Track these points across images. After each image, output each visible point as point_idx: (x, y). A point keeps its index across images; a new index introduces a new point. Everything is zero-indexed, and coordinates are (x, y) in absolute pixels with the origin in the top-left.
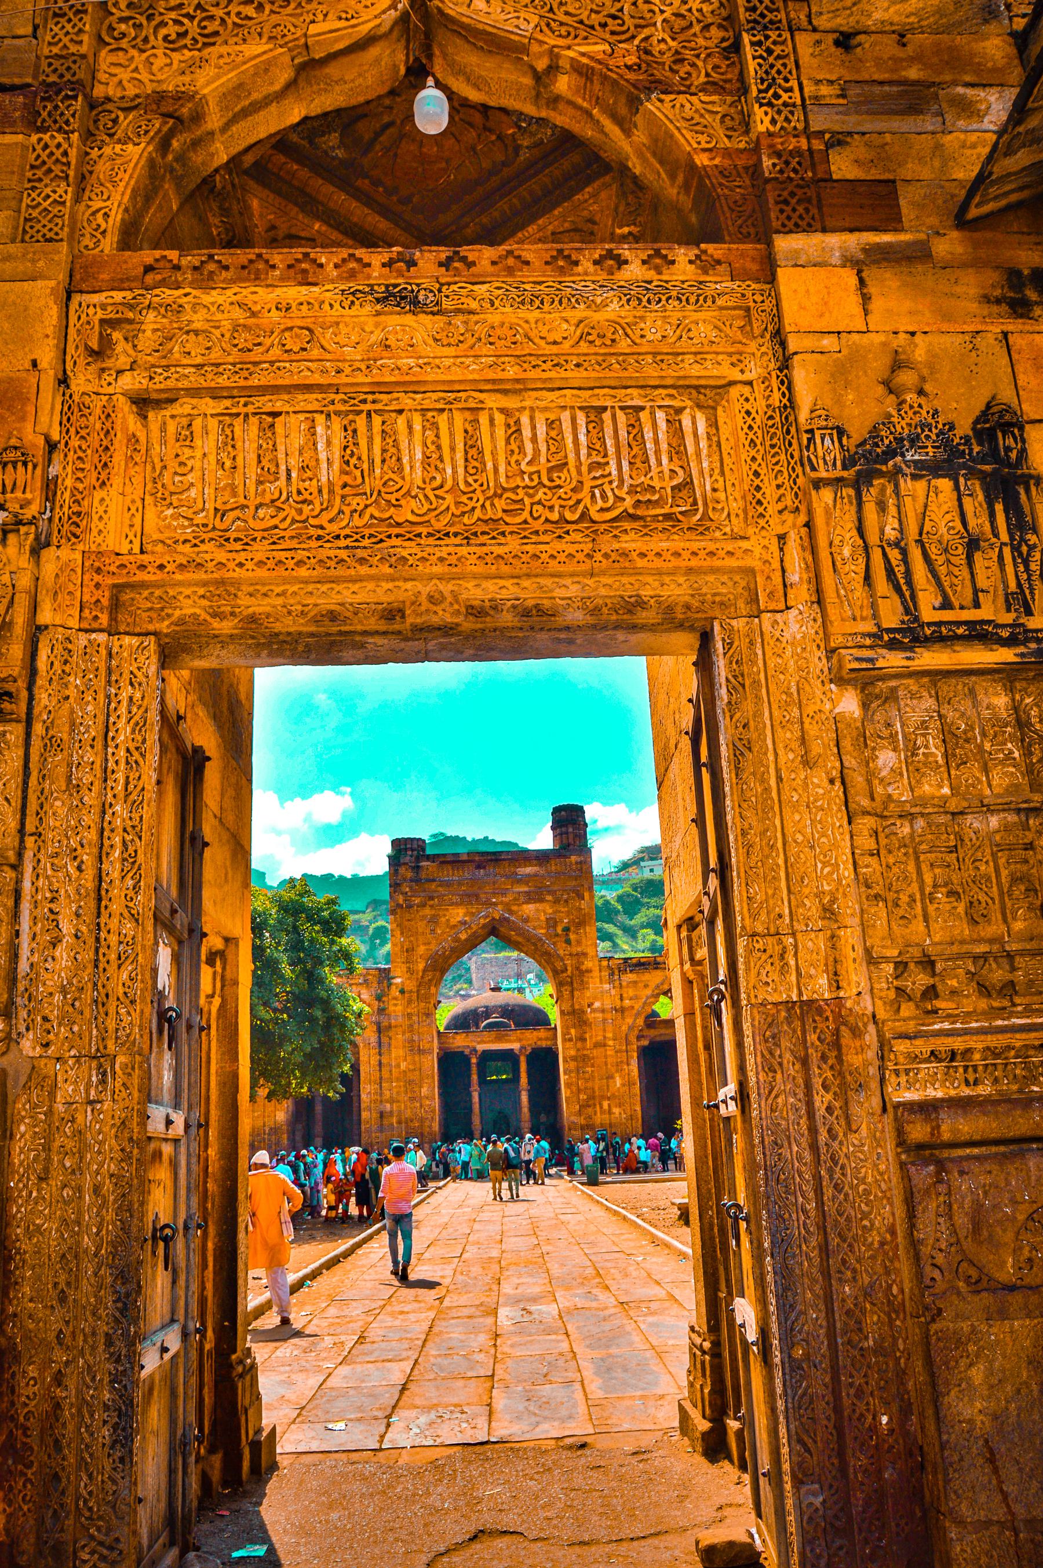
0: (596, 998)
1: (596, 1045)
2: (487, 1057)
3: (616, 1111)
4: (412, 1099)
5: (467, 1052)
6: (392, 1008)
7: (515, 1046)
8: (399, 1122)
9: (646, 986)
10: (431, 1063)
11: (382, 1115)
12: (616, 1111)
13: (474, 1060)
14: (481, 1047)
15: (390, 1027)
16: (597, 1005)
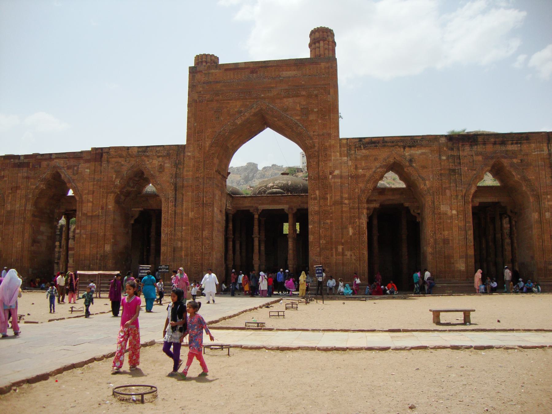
0: (336, 168)
1: (335, 203)
2: (265, 213)
3: (348, 253)
4: (196, 239)
6: (185, 173)
7: (285, 207)
8: (186, 255)
9: (376, 159)
11: (174, 250)
12: (348, 253)
13: (256, 216)
14: (261, 207)
15: (183, 187)
16: (337, 172)
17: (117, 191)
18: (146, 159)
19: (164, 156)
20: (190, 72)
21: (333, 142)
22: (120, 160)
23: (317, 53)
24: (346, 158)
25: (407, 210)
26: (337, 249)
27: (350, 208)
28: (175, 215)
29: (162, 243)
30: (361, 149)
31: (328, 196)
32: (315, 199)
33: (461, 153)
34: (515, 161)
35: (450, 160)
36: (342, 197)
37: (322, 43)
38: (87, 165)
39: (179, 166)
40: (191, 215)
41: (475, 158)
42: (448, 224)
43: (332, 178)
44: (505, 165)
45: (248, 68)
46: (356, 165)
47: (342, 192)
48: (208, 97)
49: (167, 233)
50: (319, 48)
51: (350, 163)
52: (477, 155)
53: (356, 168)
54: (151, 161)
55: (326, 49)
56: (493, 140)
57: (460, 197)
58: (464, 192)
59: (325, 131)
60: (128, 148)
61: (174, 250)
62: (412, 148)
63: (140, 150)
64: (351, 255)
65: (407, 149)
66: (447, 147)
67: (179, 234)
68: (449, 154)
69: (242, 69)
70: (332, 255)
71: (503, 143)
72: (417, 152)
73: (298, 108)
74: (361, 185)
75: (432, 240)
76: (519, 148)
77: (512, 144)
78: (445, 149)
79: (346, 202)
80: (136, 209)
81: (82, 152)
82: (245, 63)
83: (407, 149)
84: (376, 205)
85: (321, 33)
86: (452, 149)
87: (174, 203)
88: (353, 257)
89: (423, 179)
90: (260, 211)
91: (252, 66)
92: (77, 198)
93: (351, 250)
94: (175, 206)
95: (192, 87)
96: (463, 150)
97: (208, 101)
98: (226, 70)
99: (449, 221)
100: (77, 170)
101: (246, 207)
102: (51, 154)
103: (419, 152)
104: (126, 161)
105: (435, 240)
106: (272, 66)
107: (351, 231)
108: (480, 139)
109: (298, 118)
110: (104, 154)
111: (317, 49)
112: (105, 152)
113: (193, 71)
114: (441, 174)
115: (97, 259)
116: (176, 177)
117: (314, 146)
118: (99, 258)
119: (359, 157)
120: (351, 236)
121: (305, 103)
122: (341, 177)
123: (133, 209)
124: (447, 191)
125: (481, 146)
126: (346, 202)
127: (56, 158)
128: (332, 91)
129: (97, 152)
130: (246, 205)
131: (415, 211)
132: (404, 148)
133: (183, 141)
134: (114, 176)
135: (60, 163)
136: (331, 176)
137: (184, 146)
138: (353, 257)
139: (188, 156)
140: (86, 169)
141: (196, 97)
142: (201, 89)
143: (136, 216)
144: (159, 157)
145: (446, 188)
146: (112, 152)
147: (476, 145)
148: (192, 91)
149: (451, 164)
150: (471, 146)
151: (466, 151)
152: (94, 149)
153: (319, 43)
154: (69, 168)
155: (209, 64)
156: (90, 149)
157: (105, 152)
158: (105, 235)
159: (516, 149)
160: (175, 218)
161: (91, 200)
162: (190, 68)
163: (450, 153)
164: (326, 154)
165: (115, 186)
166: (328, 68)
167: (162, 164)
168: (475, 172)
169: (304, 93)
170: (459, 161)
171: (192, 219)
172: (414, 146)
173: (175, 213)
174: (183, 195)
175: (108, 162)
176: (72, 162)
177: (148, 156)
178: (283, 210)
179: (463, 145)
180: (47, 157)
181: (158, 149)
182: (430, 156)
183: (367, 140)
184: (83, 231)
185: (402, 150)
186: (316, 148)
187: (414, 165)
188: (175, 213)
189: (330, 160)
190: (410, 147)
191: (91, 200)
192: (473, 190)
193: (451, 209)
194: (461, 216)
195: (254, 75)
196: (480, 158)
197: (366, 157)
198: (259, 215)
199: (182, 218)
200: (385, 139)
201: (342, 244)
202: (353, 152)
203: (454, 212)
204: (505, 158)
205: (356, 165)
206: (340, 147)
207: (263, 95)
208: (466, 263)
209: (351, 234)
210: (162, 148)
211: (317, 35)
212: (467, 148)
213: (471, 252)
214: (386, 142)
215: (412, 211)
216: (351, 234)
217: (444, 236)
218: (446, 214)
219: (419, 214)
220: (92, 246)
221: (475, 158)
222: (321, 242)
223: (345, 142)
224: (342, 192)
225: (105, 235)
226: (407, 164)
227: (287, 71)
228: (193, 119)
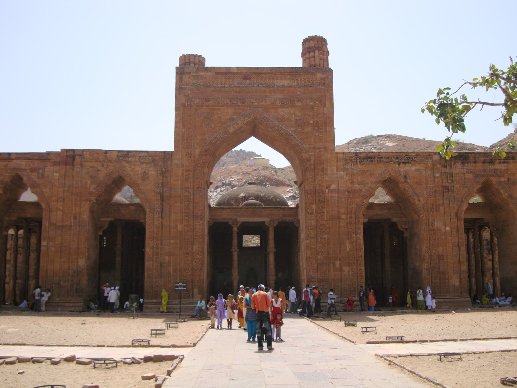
3: (346, 269)
5: (230, 222)
7: (266, 220)
8: (175, 271)
9: (371, 175)
10: (203, 228)
12: (346, 269)
13: (235, 229)
14: (241, 220)
15: (171, 197)
16: (333, 187)
17: (93, 199)
18: (127, 165)
19: (149, 163)
20: (177, 73)
21: (329, 156)
22: (95, 164)
23: (313, 63)
24: (342, 173)
25: (394, 225)
26: (334, 265)
27: (347, 224)
28: (162, 228)
29: (147, 257)
30: (357, 164)
31: (325, 211)
32: (312, 213)
33: (454, 171)
34: (502, 179)
35: (443, 177)
36: (339, 212)
37: (317, 53)
38: (57, 168)
39: (166, 175)
40: (180, 227)
41: (467, 176)
42: (440, 239)
43: (329, 192)
44: (494, 183)
45: (240, 73)
46: (352, 180)
47: (339, 207)
48: (197, 101)
49: (153, 247)
50: (314, 57)
51: (346, 178)
52: (468, 172)
53: (352, 183)
54: (133, 167)
55: (321, 59)
56: (482, 159)
57: (453, 214)
58: (457, 208)
59: (321, 144)
60: (106, 152)
61: (161, 265)
62: (407, 164)
63: (120, 154)
64: (349, 271)
65: (402, 165)
66: (440, 164)
67: (166, 247)
68: (443, 171)
69: (234, 73)
70: (329, 271)
71: (492, 162)
72: (411, 168)
73: (293, 119)
74: (357, 200)
75: (427, 256)
76: (506, 167)
77: (500, 163)
78: (438, 166)
79: (343, 216)
80: (105, 219)
81: (48, 153)
82: (238, 68)
83: (402, 165)
84: (366, 220)
85: (316, 42)
86: (445, 167)
87: (160, 215)
88: (351, 273)
89: (418, 196)
90: (239, 224)
91: (244, 71)
92: (43, 205)
93: (349, 266)
94: (162, 218)
95: (179, 89)
96: (455, 168)
97: (197, 106)
98: (217, 73)
99: (443, 237)
100: (43, 174)
101: (224, 219)
102: (10, 154)
103: (414, 168)
104: (103, 166)
105: (431, 255)
106: (265, 73)
107: (348, 247)
108: (471, 158)
109: (293, 129)
110: (77, 157)
111: (312, 59)
112: (77, 155)
113: (180, 72)
114: (435, 192)
115: (69, 275)
116: (163, 186)
117: (310, 159)
118: (71, 274)
119: (355, 172)
120: (348, 252)
121: (300, 114)
122: (338, 192)
123: (102, 219)
124: (441, 207)
125: (472, 164)
126: (343, 216)
127: (17, 159)
128: (328, 104)
129: (68, 154)
130: (224, 216)
131: (403, 226)
132: (399, 165)
133: (170, 147)
134: (89, 182)
135: (23, 164)
136: (327, 191)
137: (172, 153)
138: (351, 273)
139: (176, 164)
140: (54, 173)
141: (183, 100)
142: (189, 92)
143: (106, 226)
144: (142, 163)
145: (440, 205)
146: (86, 155)
147: (468, 163)
148: (179, 94)
149: (444, 181)
150: (463, 163)
151: (458, 168)
152: (64, 151)
153: (314, 52)
154: (32, 170)
155: (197, 66)
156: (60, 151)
157: (77, 155)
158: (78, 248)
159: (504, 168)
160: (162, 230)
161: (61, 208)
162: (177, 68)
163: (443, 170)
164: (322, 168)
165: (91, 193)
166: (324, 79)
167: (146, 171)
168: (466, 190)
169: (299, 104)
170: (451, 179)
171: (180, 232)
172: (408, 163)
173: (162, 225)
174: (170, 206)
175: (82, 166)
176: (36, 164)
177: (129, 162)
178: (264, 222)
179: (455, 163)
180: (6, 156)
181: (141, 154)
182: (424, 172)
183: (363, 155)
184: (51, 243)
185: (397, 166)
186: (312, 162)
187: (409, 181)
188: (162, 225)
189: (327, 174)
190: (405, 163)
191: (61, 208)
192: (465, 207)
193: (445, 226)
194: (454, 232)
195: (247, 81)
196: (471, 176)
197: (363, 172)
198: (238, 228)
199: (170, 231)
200: (381, 155)
201: (340, 260)
202: (349, 166)
203: (448, 228)
204: (493, 176)
205: (352, 180)
206: (337, 161)
207: (256, 104)
208: (460, 278)
209: (348, 249)
210: (146, 154)
211: (312, 43)
212: (459, 166)
213: (464, 267)
214: (382, 158)
215: (399, 227)
216: (348, 249)
217: (439, 252)
218: (440, 230)
219: (406, 229)
220: (63, 260)
221: (467, 176)
222: (319, 257)
223: (341, 156)
224: (339, 207)
225: (78, 248)
226: (403, 180)
227: (281, 79)
228: (181, 125)
